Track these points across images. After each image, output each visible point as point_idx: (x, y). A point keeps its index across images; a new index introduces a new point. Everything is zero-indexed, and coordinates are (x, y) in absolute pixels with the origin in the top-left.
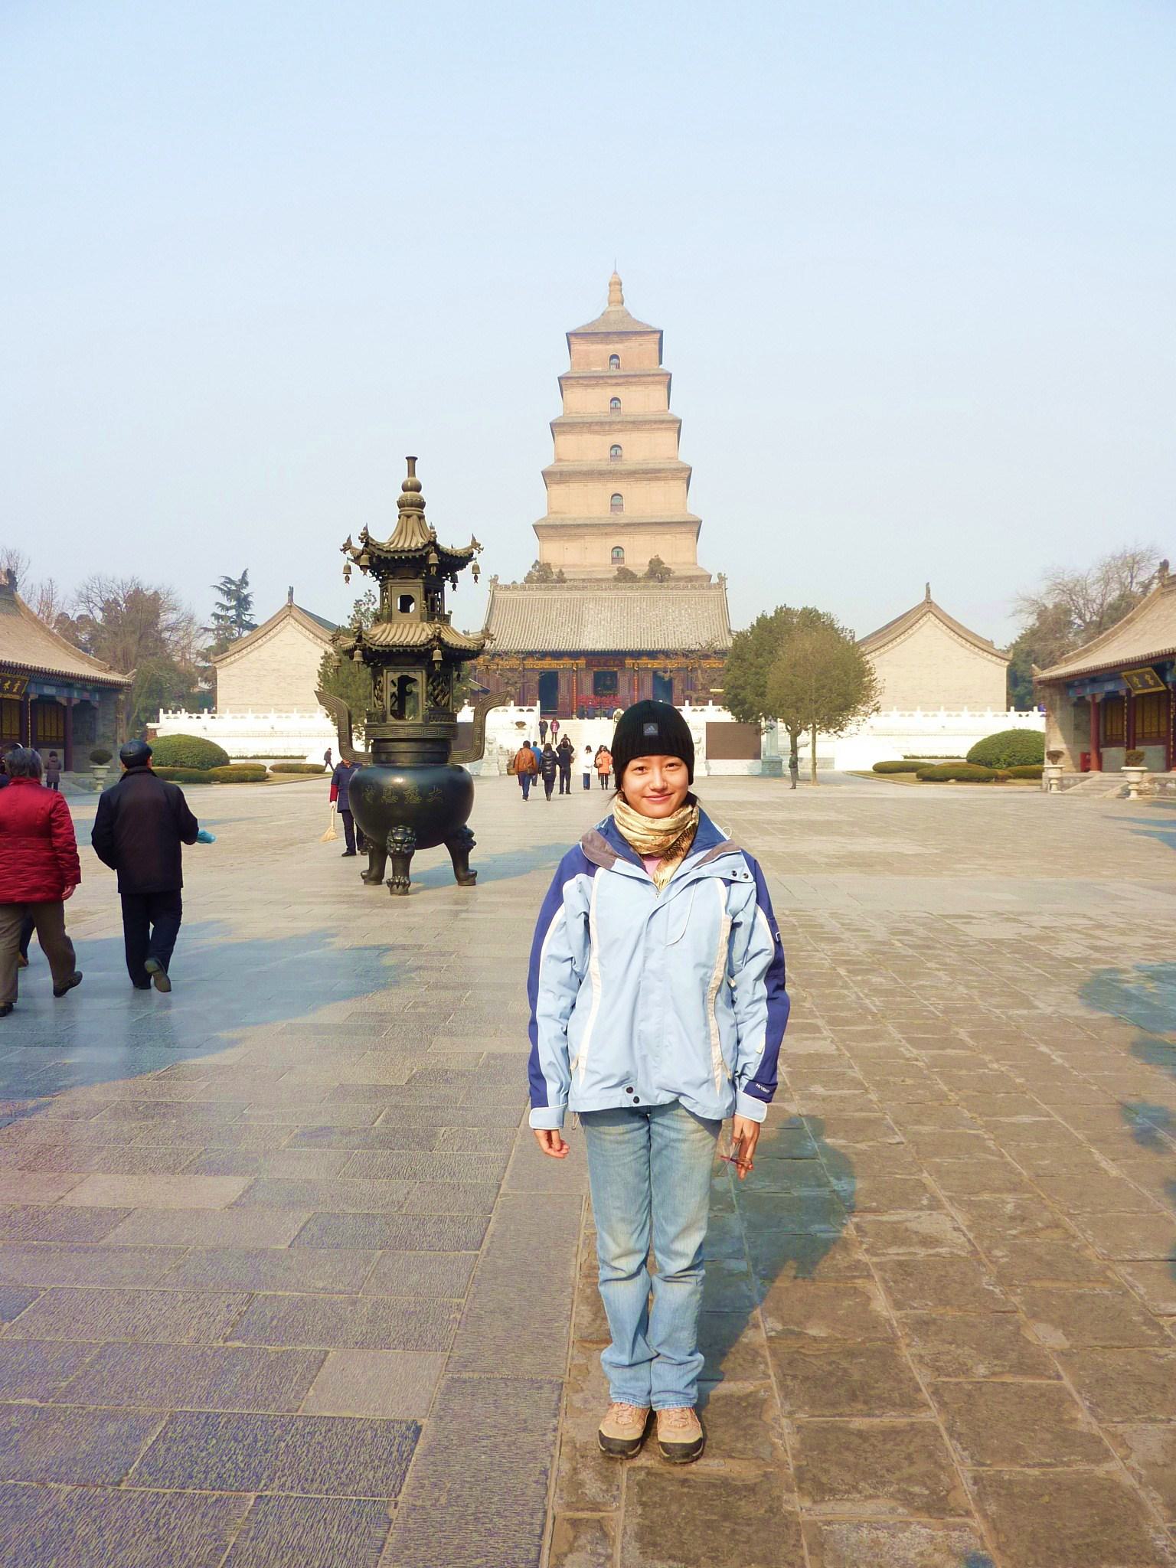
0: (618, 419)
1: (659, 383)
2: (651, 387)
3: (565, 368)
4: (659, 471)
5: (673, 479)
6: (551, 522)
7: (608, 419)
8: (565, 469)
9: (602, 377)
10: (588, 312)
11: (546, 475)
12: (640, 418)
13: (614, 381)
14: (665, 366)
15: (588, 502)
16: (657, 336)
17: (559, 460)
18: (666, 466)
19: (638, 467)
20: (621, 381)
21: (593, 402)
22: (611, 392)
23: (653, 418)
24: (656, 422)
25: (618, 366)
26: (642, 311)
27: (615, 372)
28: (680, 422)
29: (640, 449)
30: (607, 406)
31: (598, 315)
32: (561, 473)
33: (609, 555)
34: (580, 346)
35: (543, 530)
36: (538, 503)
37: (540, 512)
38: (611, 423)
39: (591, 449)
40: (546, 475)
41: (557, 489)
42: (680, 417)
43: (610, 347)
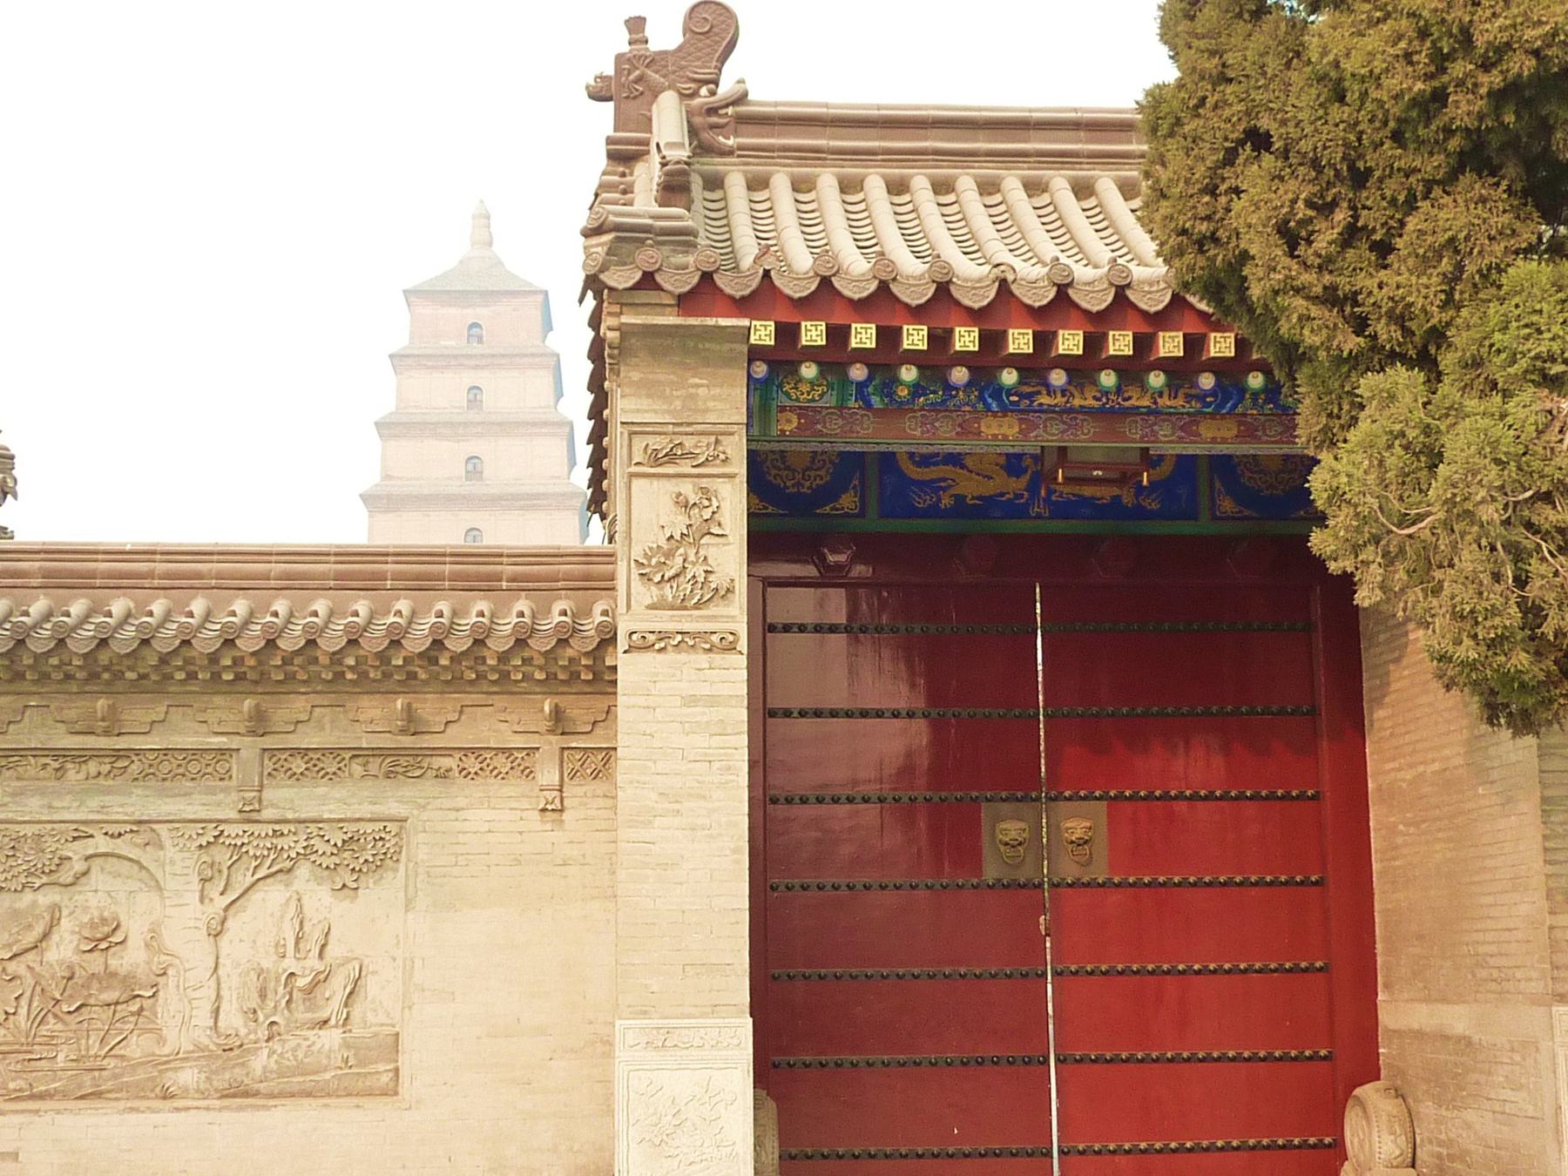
0: (479, 418)
4: (537, 496)
9: (456, 357)
10: (441, 254)
11: (366, 498)
13: (473, 363)
16: (540, 298)
17: (387, 477)
21: (442, 392)
22: (468, 378)
24: (535, 424)
25: (480, 340)
27: (476, 349)
32: (389, 497)
40: (366, 498)
43: (469, 311)
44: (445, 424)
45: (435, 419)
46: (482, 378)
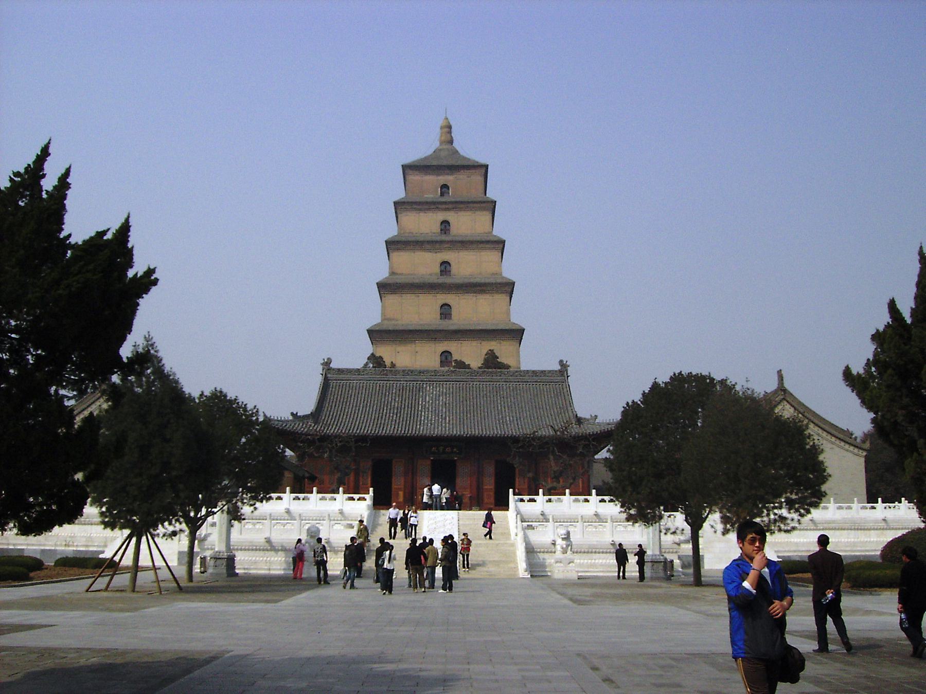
1: (484, 209)
2: (478, 213)
3: (400, 194)
4: (485, 285)
5: (497, 292)
6: (384, 328)
7: (438, 239)
8: (399, 281)
9: (434, 203)
12: (467, 239)
13: (444, 206)
14: (490, 194)
15: (421, 311)
17: (393, 273)
18: (492, 280)
19: (466, 281)
20: (450, 206)
21: (426, 224)
22: (441, 216)
23: (478, 239)
24: (482, 242)
26: (469, 147)
28: (502, 243)
29: (467, 265)
30: (436, 228)
31: (430, 152)
33: (438, 359)
34: (414, 177)
35: (376, 335)
36: (372, 310)
37: (374, 318)
38: (441, 242)
39: (423, 265)
41: (392, 299)
42: (503, 237)
43: (440, 178)
44: (428, 242)
45: (422, 239)
46: (450, 216)
